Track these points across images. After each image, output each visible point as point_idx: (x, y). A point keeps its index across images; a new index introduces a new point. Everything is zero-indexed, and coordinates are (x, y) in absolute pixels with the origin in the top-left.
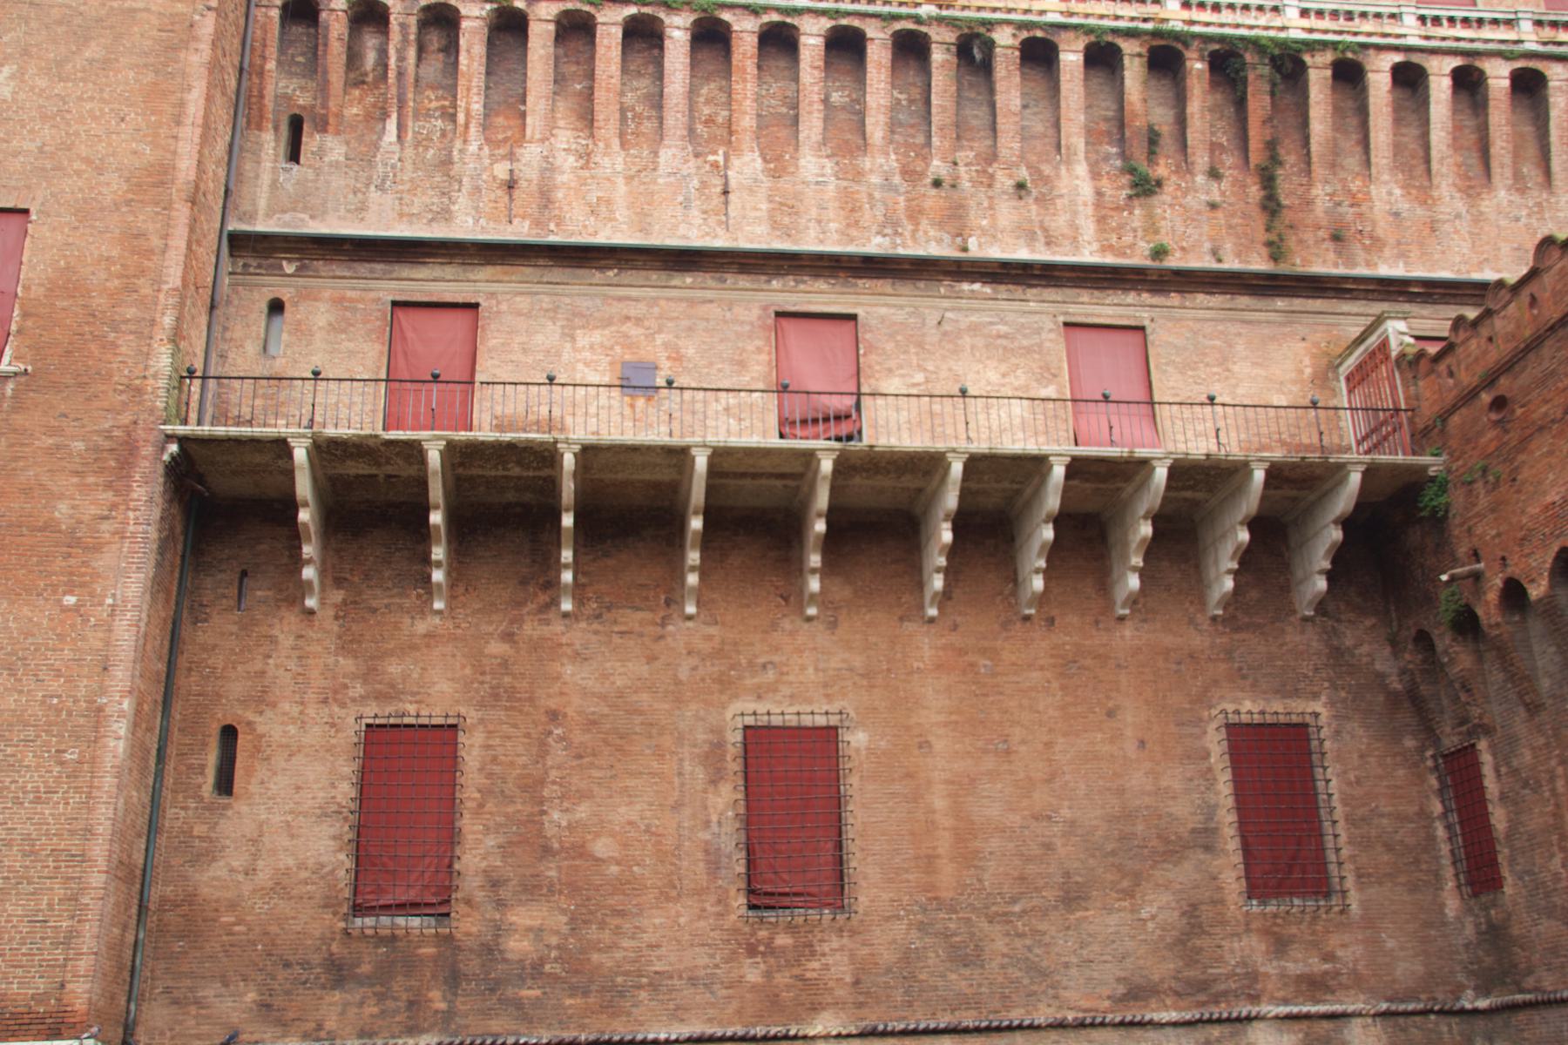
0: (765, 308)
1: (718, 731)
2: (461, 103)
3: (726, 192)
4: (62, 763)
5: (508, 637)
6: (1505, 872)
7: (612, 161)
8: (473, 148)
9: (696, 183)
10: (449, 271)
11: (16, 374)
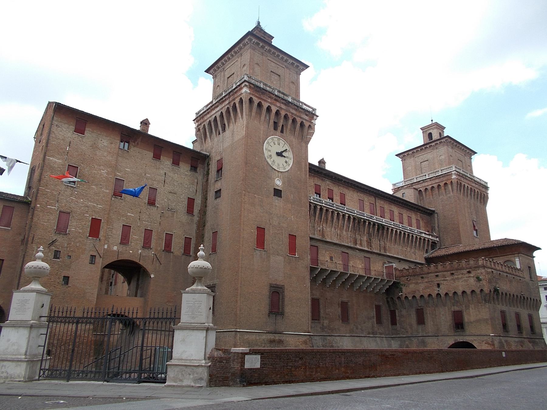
5: (322, 289)
7: (328, 229)
9: (335, 233)
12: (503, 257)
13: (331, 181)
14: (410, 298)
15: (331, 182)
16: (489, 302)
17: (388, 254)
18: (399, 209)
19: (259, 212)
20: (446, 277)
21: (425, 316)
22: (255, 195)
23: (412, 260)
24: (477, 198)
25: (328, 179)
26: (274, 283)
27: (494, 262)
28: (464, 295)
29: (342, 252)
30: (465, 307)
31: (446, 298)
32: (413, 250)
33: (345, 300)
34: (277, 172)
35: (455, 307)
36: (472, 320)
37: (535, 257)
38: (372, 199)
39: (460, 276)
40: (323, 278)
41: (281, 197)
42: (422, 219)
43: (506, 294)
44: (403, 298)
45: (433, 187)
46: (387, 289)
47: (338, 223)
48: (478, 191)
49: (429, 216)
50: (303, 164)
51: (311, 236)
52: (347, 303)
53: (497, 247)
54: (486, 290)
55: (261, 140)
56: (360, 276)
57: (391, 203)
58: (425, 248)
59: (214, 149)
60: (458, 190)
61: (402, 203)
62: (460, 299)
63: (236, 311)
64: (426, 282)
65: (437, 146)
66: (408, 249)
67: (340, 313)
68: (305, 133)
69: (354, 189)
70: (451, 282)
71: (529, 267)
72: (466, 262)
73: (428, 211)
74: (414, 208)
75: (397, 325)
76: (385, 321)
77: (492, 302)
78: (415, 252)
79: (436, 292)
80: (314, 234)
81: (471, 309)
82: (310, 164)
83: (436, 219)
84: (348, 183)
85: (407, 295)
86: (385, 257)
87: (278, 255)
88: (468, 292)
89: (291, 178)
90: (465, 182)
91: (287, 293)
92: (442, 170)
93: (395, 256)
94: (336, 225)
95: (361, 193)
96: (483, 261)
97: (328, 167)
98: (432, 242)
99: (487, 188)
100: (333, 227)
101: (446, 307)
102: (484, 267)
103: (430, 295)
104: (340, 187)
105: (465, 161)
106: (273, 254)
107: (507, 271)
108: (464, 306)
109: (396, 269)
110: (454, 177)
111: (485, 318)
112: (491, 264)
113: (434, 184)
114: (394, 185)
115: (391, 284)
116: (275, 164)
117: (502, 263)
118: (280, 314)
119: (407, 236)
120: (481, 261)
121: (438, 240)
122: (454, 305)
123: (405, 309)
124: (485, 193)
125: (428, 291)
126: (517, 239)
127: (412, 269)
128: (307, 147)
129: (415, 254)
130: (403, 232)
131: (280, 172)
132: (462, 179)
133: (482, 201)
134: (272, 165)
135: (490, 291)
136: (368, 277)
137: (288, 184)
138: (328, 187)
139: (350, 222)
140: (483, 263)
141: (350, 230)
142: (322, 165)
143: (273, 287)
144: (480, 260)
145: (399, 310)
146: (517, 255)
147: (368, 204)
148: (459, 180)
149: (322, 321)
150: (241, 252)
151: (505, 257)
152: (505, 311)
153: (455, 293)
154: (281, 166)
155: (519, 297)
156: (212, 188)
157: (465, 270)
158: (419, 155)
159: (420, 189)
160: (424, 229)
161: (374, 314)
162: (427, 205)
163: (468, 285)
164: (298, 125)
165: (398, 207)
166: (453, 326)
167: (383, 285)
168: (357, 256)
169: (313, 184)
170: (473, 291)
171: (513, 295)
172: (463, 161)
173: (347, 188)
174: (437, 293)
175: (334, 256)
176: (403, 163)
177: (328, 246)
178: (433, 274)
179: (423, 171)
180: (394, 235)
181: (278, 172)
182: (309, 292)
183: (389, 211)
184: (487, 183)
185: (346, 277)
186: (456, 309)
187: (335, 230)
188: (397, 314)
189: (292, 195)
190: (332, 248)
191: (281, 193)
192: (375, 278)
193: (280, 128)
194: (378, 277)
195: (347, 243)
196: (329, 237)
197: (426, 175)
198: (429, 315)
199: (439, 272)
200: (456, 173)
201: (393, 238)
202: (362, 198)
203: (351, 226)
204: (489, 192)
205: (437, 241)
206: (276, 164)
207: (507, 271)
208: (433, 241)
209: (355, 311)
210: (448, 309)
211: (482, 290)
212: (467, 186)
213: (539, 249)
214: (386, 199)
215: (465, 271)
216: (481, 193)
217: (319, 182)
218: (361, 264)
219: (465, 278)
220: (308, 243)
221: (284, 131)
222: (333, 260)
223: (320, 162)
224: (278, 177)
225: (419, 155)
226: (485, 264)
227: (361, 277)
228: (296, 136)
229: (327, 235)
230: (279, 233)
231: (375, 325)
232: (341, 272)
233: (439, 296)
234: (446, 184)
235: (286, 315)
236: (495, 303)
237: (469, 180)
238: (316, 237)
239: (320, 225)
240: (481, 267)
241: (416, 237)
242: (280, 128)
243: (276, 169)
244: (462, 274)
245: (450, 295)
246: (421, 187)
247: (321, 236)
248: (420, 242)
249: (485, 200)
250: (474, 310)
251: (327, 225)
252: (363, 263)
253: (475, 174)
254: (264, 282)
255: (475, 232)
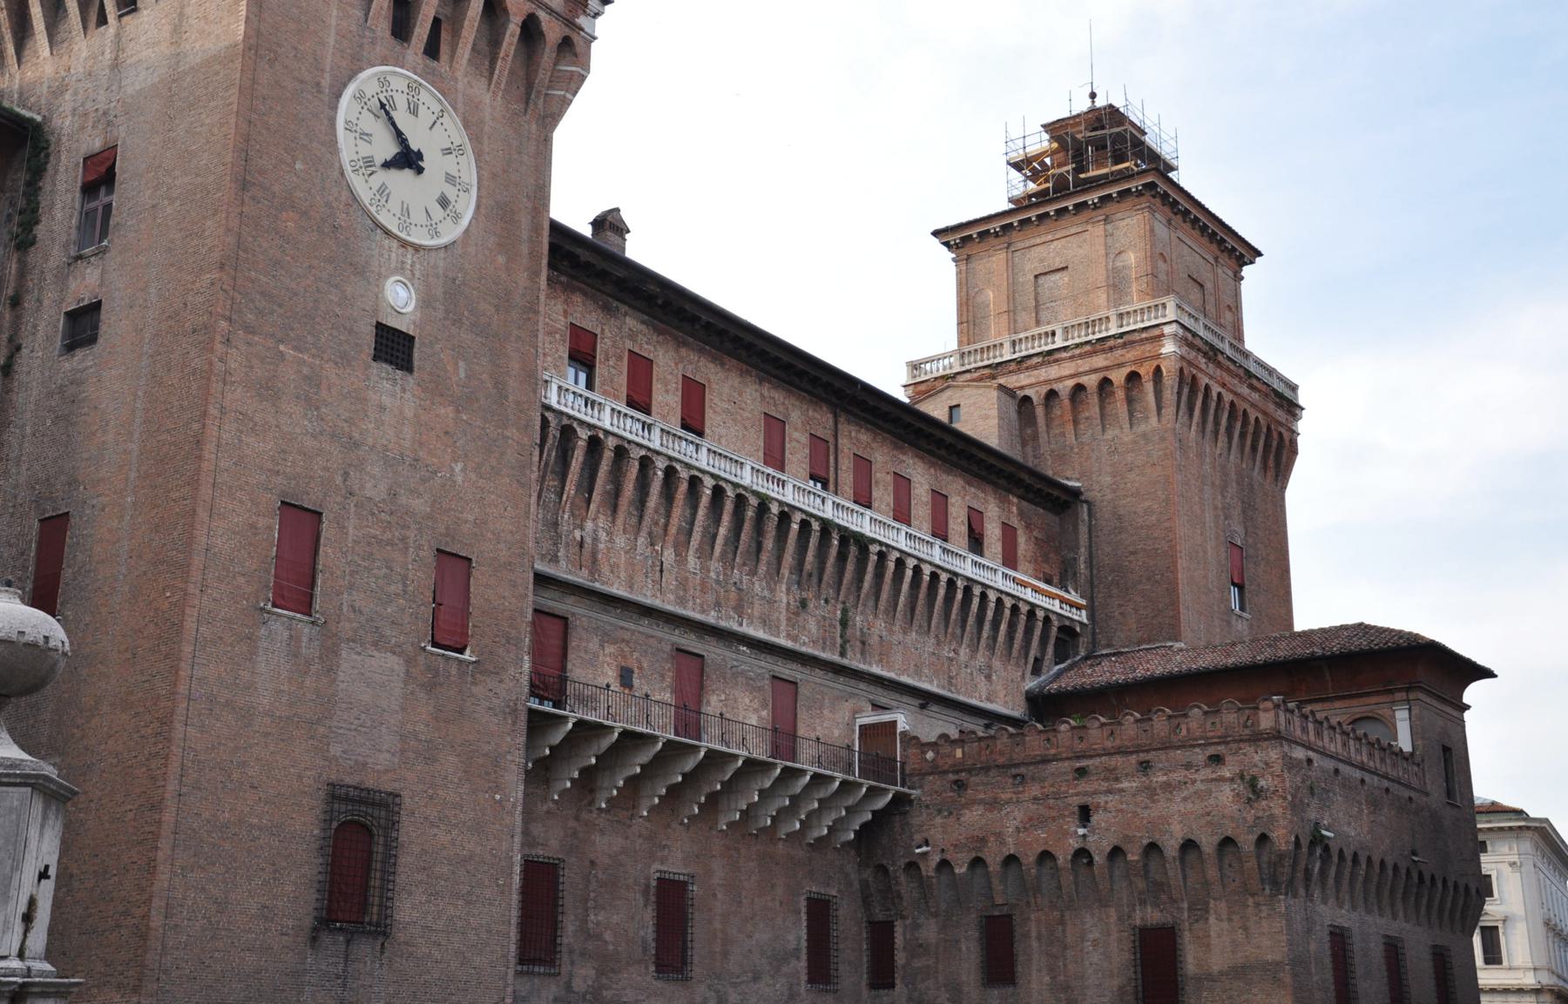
0: (673, 645)
1: (648, 879)
2: (567, 488)
3: (661, 571)
4: (498, 886)
5: (577, 818)
6: (898, 981)
7: (621, 541)
8: (566, 516)
9: (650, 562)
10: (557, 595)
11: (475, 662)
12: (1346, 703)
13: (646, 317)
14: (961, 870)
15: (643, 322)
16: (1291, 889)
17: (876, 670)
18: (932, 470)
19: (298, 431)
20: (1117, 780)
21: (1019, 948)
22: (282, 347)
23: (974, 702)
24: (1254, 448)
25: (630, 306)
26: (348, 780)
27: (1316, 721)
28: (1191, 856)
29: (679, 650)
30: (1190, 909)
31: (1111, 869)
32: (981, 658)
33: (675, 867)
34: (395, 244)
35: (1149, 909)
36: (1216, 969)
37: (1468, 707)
38: (822, 420)
39: (1177, 776)
40: (585, 764)
41: (406, 365)
42: (1028, 526)
43: (1355, 855)
44: (929, 868)
45: (1079, 388)
46: (864, 826)
47: (668, 515)
48: (1257, 418)
49: (1057, 514)
50: (525, 220)
51: (541, 567)
52: (685, 883)
53: (1324, 658)
54: (1281, 838)
55: (327, 76)
56: (750, 763)
57: (900, 443)
58: (1033, 654)
59: (67, 96)
60: (1183, 405)
61: (950, 447)
62: (1171, 874)
63: (146, 916)
64: (1035, 798)
65: (1110, 208)
66: (964, 652)
67: (651, 929)
68: (543, 76)
69: (745, 367)
70: (1139, 799)
71: (1446, 750)
72: (1206, 713)
73: (1056, 493)
74: (999, 473)
75: (892, 986)
76: (844, 969)
77: (1302, 892)
78: (990, 667)
79: (1074, 844)
80: (554, 559)
81: (1212, 919)
82: (557, 229)
83: (1083, 529)
84: (721, 333)
85: (948, 857)
86: (862, 686)
87: (375, 644)
88: (1208, 842)
89: (464, 283)
90: (1211, 377)
91: (408, 831)
92: (1121, 316)
93: (905, 679)
94: (656, 524)
95: (776, 388)
96: (1277, 716)
97: (638, 250)
98: (1062, 629)
99: (1292, 408)
100: (644, 533)
101: (1112, 912)
102: (1276, 736)
103: (1046, 856)
104: (683, 351)
105: (1216, 287)
106: (353, 641)
107: (1365, 760)
108: (1185, 905)
109: (910, 740)
110: (1169, 348)
111: (1269, 958)
112: (1305, 730)
113: (1086, 373)
114: (915, 366)
115: (881, 803)
116: (388, 206)
117: (1348, 728)
118: (370, 933)
119: (959, 596)
120: (1267, 715)
121: (1085, 621)
122: (1143, 903)
123: (936, 915)
124: (1283, 430)
125: (1041, 838)
126: (1407, 629)
127: (981, 739)
128: (545, 143)
129: (988, 677)
130: (944, 577)
131: (413, 245)
132: (1202, 361)
133: (1271, 463)
134: (373, 210)
135: (1297, 843)
136: (785, 770)
137: (447, 312)
138: (629, 345)
139: (721, 515)
140: (1277, 721)
141: (718, 549)
142: (612, 237)
143: (347, 799)
144: (1266, 710)
145: (908, 922)
146: (1402, 695)
147: (804, 439)
148: (1190, 363)
149: (564, 970)
150: (190, 624)
151: (1355, 702)
152: (1348, 929)
153: (1153, 848)
154: (418, 216)
155: (1403, 871)
156: (49, 296)
157: (1197, 750)
158: (1032, 242)
159: (1028, 392)
160: (1030, 567)
161: (799, 939)
162: (1049, 463)
163: (1208, 814)
164: (513, 29)
165: (933, 465)
166: (1136, 993)
167: (847, 809)
168: (743, 673)
169: (561, 323)
170: (1227, 842)
171: (1382, 862)
172: (1209, 285)
173: (714, 359)
174: (1077, 846)
175: (641, 668)
176: (959, 273)
177: (613, 620)
178: (1066, 764)
179: (1044, 315)
180: (905, 586)
181: (404, 244)
182: (518, 830)
183: (890, 478)
184: (1294, 388)
185: (690, 764)
186: (1152, 916)
187: (652, 544)
188: (899, 941)
189: (461, 364)
190: (633, 626)
191: (411, 348)
192: (815, 776)
193: (421, 31)
194: (828, 773)
195: (703, 611)
196: (623, 575)
197: (1053, 334)
198: (1035, 944)
199: (1091, 757)
200: (1181, 331)
201: (902, 599)
202: (781, 408)
203: (722, 531)
204: (1302, 426)
205: (1081, 623)
206: (393, 204)
207: (1365, 760)
208: (1067, 623)
209: (718, 926)
210: (1119, 919)
211: (1263, 839)
212: (1219, 394)
213: (1487, 673)
214: (881, 423)
215: (1199, 756)
216: (1269, 428)
217: (590, 319)
218: (756, 710)
219: (1199, 786)
220: (528, 600)
221: (444, 49)
222: (631, 687)
223: (599, 223)
224: (400, 269)
225: (1032, 242)
226: (1282, 728)
227: (753, 767)
228: (498, 83)
229: (614, 568)
230: (390, 543)
231: (803, 986)
232: (669, 743)
233: (1085, 861)
234: (1133, 377)
235: (401, 937)
236: (1309, 896)
237: (1228, 370)
238: (562, 571)
239: (583, 520)
240: (1266, 739)
241: (999, 601)
242: (421, 31)
243: (395, 230)
244: (1188, 766)
245: (1130, 857)
246: (1031, 386)
247: (585, 572)
248: (1012, 626)
249: (1284, 459)
250: (1225, 925)
251: (613, 522)
252: (764, 706)
253: (1252, 343)
254: (300, 777)
255: (1234, 592)
